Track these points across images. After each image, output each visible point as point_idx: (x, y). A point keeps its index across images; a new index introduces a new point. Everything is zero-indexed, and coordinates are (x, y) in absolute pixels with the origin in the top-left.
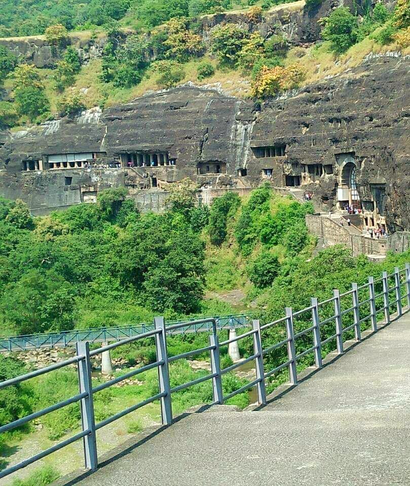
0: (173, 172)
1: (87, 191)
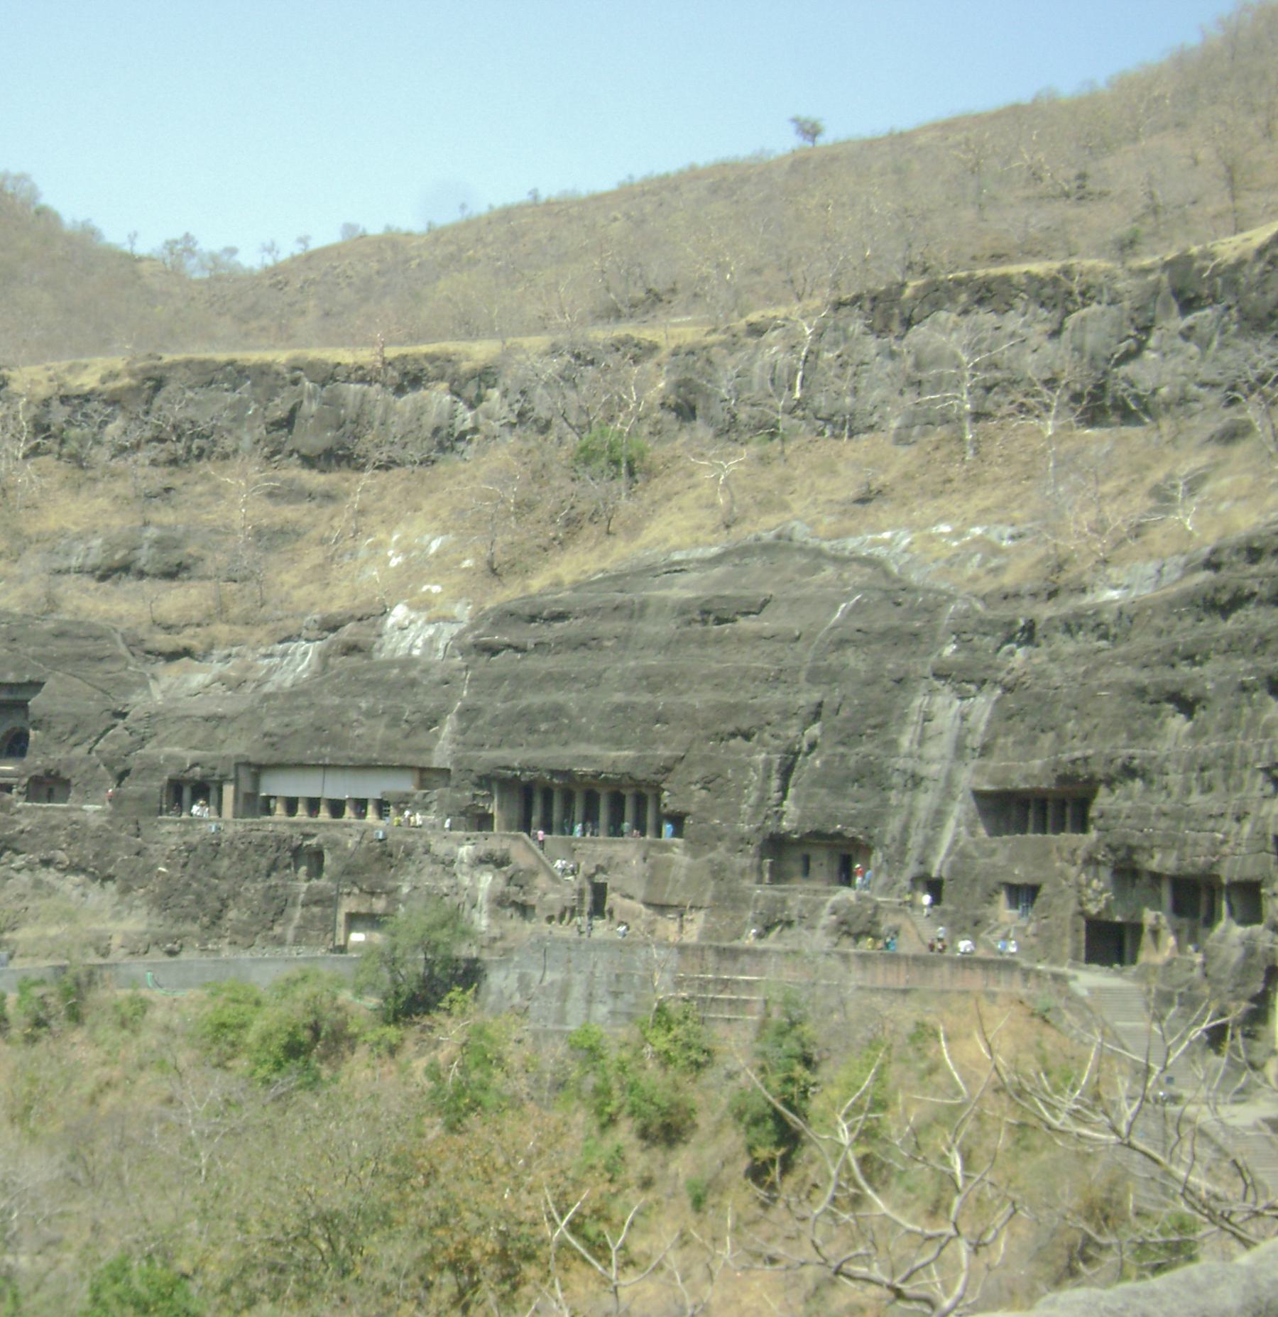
0: (669, 864)
1: (363, 910)
